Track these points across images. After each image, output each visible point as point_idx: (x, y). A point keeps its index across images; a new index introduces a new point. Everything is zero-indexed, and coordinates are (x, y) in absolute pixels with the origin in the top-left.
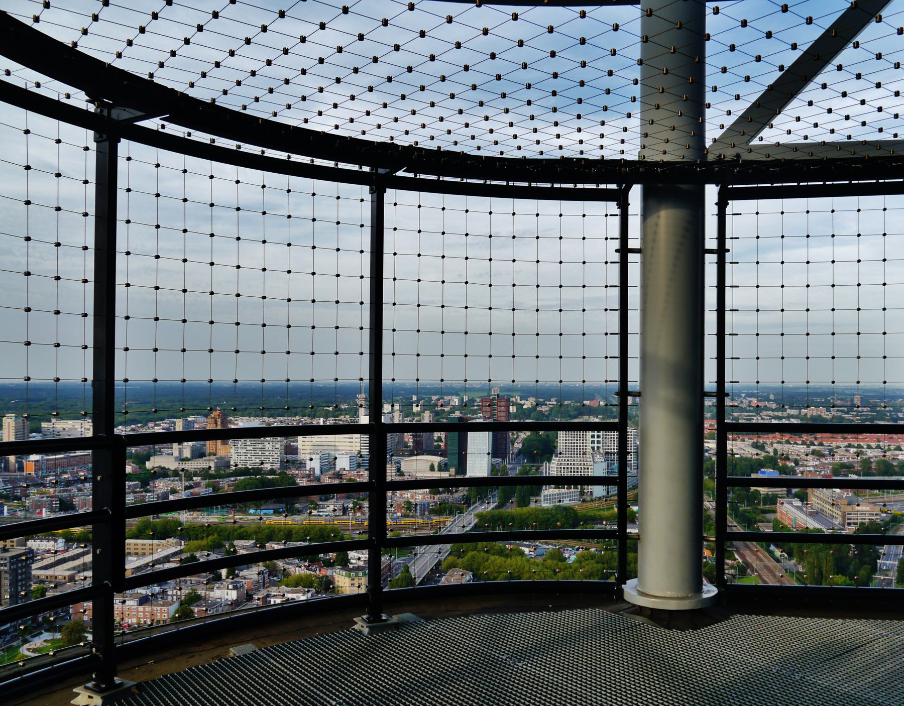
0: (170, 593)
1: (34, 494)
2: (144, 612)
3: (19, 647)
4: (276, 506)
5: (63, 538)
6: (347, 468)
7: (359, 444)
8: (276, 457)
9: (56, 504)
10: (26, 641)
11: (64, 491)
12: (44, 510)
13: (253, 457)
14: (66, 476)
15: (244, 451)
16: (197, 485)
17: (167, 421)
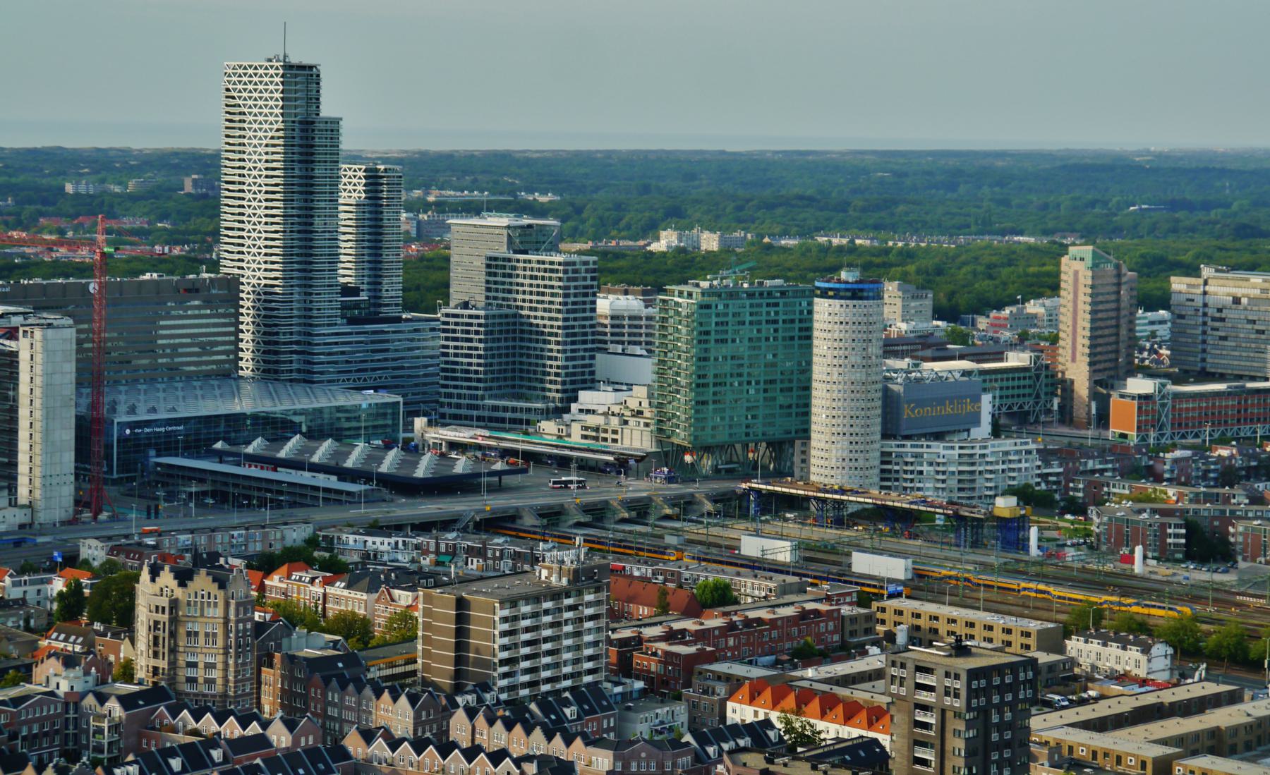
5: (1167, 643)
9: (1176, 536)
11: (1208, 498)
12: (1139, 550)
14: (1224, 452)
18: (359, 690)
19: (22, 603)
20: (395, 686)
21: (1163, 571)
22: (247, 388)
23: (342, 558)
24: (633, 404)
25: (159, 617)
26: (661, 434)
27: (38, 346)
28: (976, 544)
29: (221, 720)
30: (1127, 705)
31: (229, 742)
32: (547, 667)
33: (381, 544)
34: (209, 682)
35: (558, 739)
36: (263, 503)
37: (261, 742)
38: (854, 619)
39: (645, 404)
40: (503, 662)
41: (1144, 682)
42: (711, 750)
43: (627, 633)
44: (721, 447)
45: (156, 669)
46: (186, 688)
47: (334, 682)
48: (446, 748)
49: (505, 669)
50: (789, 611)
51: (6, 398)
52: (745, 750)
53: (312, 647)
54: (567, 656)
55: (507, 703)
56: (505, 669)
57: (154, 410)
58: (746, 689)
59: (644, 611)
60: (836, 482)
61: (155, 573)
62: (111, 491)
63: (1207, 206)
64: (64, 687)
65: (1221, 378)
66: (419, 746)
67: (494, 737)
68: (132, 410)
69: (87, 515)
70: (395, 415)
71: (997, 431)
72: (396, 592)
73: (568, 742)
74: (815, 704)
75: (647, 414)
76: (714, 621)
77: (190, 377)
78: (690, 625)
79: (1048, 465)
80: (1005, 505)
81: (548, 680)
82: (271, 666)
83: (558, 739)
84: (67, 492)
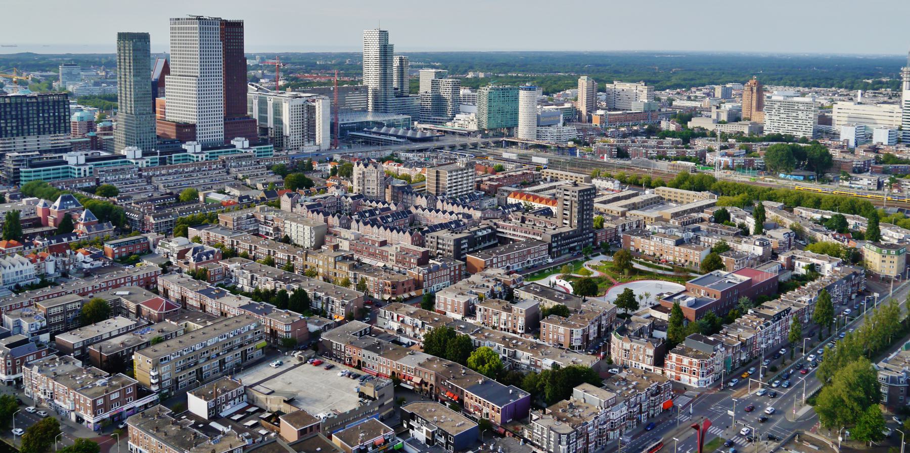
0: (702, 239)
1: (599, 142)
2: (680, 252)
3: (583, 262)
4: (807, 173)
6: (885, 142)
7: (901, 119)
8: (809, 125)
9: (615, 152)
10: (587, 259)
11: (621, 141)
13: (786, 125)
14: (623, 129)
15: (778, 118)
16: (732, 146)
17: (707, 87)
19: (321, 171)
20: (420, 193)
21: (612, 161)
22: (370, 114)
24: (471, 118)
26: (479, 124)
28: (563, 154)
30: (611, 197)
33: (410, 155)
34: (373, 193)
36: (378, 144)
37: (388, 209)
38: (536, 175)
40: (449, 187)
41: (613, 191)
42: (506, 211)
44: (495, 129)
46: (367, 194)
48: (437, 211)
50: (520, 173)
53: (399, 183)
54: (465, 186)
58: (513, 193)
59: (480, 173)
60: (525, 138)
62: (339, 141)
63: (605, 65)
64: (337, 194)
65: (619, 110)
66: (430, 210)
67: (449, 208)
68: (343, 120)
69: (333, 148)
71: (564, 125)
74: (531, 198)
76: (500, 176)
77: (356, 111)
78: (494, 177)
79: (579, 133)
80: (571, 144)
84: (328, 142)
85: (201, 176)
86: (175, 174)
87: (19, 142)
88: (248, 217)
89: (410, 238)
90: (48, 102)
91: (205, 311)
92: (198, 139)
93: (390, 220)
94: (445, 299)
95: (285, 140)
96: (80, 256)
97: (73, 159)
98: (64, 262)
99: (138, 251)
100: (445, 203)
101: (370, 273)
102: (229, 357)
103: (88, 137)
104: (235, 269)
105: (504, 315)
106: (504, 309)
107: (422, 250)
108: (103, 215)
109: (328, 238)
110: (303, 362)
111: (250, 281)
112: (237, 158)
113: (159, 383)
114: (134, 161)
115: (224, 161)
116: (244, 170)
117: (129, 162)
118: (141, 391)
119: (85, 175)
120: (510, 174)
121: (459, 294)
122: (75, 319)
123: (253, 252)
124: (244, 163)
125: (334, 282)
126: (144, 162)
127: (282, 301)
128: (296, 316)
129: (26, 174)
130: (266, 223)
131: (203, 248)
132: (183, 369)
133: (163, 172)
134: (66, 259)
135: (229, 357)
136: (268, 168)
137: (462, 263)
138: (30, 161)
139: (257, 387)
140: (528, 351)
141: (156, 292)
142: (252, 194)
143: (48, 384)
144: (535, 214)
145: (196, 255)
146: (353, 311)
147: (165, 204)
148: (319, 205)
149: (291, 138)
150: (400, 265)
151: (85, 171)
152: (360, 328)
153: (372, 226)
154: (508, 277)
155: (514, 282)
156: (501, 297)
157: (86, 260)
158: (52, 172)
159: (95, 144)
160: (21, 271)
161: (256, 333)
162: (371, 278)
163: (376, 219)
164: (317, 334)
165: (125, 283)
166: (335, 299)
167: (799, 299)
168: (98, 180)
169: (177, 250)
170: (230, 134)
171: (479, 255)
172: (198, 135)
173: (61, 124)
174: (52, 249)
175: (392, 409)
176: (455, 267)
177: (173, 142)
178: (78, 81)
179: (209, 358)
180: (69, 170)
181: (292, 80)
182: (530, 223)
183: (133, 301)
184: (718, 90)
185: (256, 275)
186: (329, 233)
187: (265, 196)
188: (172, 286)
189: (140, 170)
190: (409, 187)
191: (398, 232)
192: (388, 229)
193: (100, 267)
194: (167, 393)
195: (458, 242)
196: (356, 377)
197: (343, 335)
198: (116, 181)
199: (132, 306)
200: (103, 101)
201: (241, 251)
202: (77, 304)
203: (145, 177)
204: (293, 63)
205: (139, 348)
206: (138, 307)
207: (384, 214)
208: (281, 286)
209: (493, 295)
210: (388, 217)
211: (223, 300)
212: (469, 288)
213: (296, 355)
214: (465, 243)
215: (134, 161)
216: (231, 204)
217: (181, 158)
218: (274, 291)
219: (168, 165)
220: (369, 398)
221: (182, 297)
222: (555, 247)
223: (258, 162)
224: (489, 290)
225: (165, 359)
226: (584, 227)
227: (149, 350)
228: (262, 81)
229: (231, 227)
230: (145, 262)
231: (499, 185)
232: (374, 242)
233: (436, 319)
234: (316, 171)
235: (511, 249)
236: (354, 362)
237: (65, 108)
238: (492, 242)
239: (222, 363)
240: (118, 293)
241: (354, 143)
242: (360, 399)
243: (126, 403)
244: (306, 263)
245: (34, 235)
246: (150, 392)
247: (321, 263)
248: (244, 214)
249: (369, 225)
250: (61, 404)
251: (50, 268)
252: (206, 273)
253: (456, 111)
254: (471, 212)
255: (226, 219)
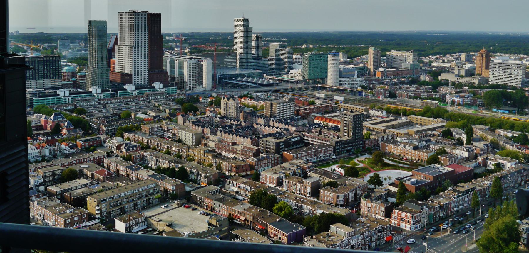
0: (431, 146)
1: (378, 88)
2: (415, 154)
4: (511, 109)
5: (385, 111)
8: (519, 79)
9: (387, 94)
11: (392, 88)
12: (381, 96)
13: (504, 78)
14: (395, 80)
15: (498, 74)
16: (465, 91)
17: (457, 54)
18: (256, 117)
19: (204, 102)
20: (261, 116)
21: (385, 99)
22: (238, 69)
23: (253, 96)
24: (299, 72)
25: (225, 105)
27: (206, 63)
28: (355, 95)
29: (234, 121)
30: (379, 121)
31: (236, 125)
32: (285, 114)
33: (259, 94)
34: (232, 115)
35: (287, 125)
36: (240, 88)
37: (240, 125)
38: (334, 107)
39: (301, 72)
40: (278, 113)
41: (382, 117)
42: (311, 127)
43: (298, 109)
45: (224, 113)
46: (229, 116)
47: (252, 116)
48: (269, 126)
49: (278, 114)
50: (324, 105)
51: (201, 71)
52: (317, 127)
53: (248, 110)
54: (288, 112)
55: (279, 119)
56: (278, 114)
57: (224, 73)
59: (300, 105)
60: (332, 85)
61: (224, 98)
62: (217, 86)
63: (392, 40)
64: (210, 116)
65: (395, 68)
66: (265, 126)
67: (277, 125)
68: (220, 73)
69: (213, 89)
70: (261, 74)
71: (358, 77)
72: (261, 102)
73: (288, 126)
74: (328, 120)
75: (301, 74)
76: (312, 107)
77: (229, 68)
78: (308, 107)
79: (366, 82)
80: (359, 89)
81: (285, 116)
82: (242, 113)
83: (287, 125)
84: (210, 85)
85: (134, 104)
86: (119, 103)
87: (34, 83)
88: (158, 127)
89: (250, 142)
90: (49, 60)
91: (129, 178)
92: (134, 83)
93: (240, 131)
94: (266, 176)
95: (185, 84)
96: (63, 146)
97: (62, 93)
98: (54, 149)
99: (95, 145)
100: (275, 122)
101: (224, 160)
102: (139, 202)
103: (72, 81)
104: (147, 156)
105: (299, 186)
106: (299, 182)
107: (256, 148)
108: (77, 124)
109: (202, 140)
110: (180, 205)
111: (155, 163)
112: (155, 94)
113: (100, 213)
114: (96, 95)
115: (147, 96)
116: (159, 101)
117: (93, 95)
118: (90, 217)
119: (69, 102)
120: (318, 106)
121: (274, 173)
122: (58, 179)
123: (159, 147)
124: (159, 97)
125: (204, 165)
126: (102, 96)
127: (171, 173)
128: (178, 181)
129: (37, 101)
130: (168, 131)
131: (130, 144)
132: (114, 206)
133: (112, 101)
134: (56, 148)
135: (139, 202)
136: (173, 100)
137: (279, 156)
138: (39, 94)
139: (153, 218)
140: (309, 205)
141: (104, 167)
142: (162, 115)
143: (42, 211)
144: (328, 129)
145: (126, 148)
146: (212, 181)
147: (112, 119)
148: (200, 121)
149: (189, 83)
150: (243, 157)
151: (69, 100)
152: (214, 189)
153: (229, 134)
154: (305, 164)
155: (309, 168)
156: (300, 176)
157: (66, 149)
158: (50, 100)
159: (75, 85)
160: (31, 153)
161: (155, 190)
162: (224, 163)
163: (232, 130)
164: (190, 192)
165: (86, 162)
166: (202, 173)
167: (484, 183)
168: (75, 105)
169: (116, 144)
170: (152, 80)
171: (290, 151)
172: (134, 81)
173: (56, 73)
174: (48, 142)
175: (227, 233)
176: (274, 158)
177: (119, 84)
178: (69, 49)
179: (128, 202)
180: (60, 99)
181: (193, 49)
182: (324, 135)
183: (90, 171)
184: (463, 56)
185: (159, 159)
186: (203, 137)
187: (169, 116)
188: (112, 164)
189: (99, 100)
190: (254, 112)
191: (244, 138)
192: (238, 136)
193: (74, 153)
194: (104, 220)
195: (278, 144)
196: (208, 215)
197: (204, 193)
198: (85, 106)
199: (89, 174)
200: (82, 61)
201: (152, 146)
202: (60, 171)
203: (102, 104)
204: (196, 39)
205: (91, 194)
206: (93, 174)
207: (237, 128)
208: (173, 165)
209: (295, 174)
210: (240, 129)
211: (139, 172)
212: (281, 170)
213: (176, 202)
214: (282, 145)
215: (96, 95)
216: (149, 120)
217: (123, 94)
218: (168, 168)
219: (116, 97)
220: (214, 226)
221: (117, 170)
222: (338, 149)
223: (167, 97)
224: (293, 171)
225: (104, 200)
226: (357, 137)
227: (95, 196)
228: (176, 49)
229: (148, 133)
230: (99, 151)
231: (310, 113)
232: (229, 143)
233: (258, 186)
234: (201, 103)
235: (310, 149)
236: (209, 208)
237: (58, 64)
238: (301, 145)
239: (136, 205)
240: (82, 166)
241: (226, 87)
242: (209, 226)
243: (82, 223)
244: (188, 154)
245: (39, 135)
246: (95, 218)
247: (196, 154)
248: (155, 126)
249: (227, 133)
250: (49, 222)
251: (47, 152)
252: (131, 157)
253: (291, 68)
254: (290, 127)
255: (146, 128)
